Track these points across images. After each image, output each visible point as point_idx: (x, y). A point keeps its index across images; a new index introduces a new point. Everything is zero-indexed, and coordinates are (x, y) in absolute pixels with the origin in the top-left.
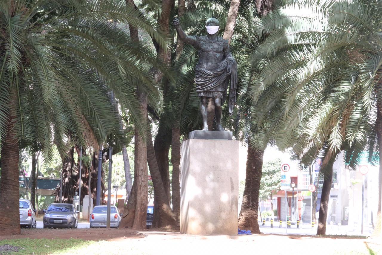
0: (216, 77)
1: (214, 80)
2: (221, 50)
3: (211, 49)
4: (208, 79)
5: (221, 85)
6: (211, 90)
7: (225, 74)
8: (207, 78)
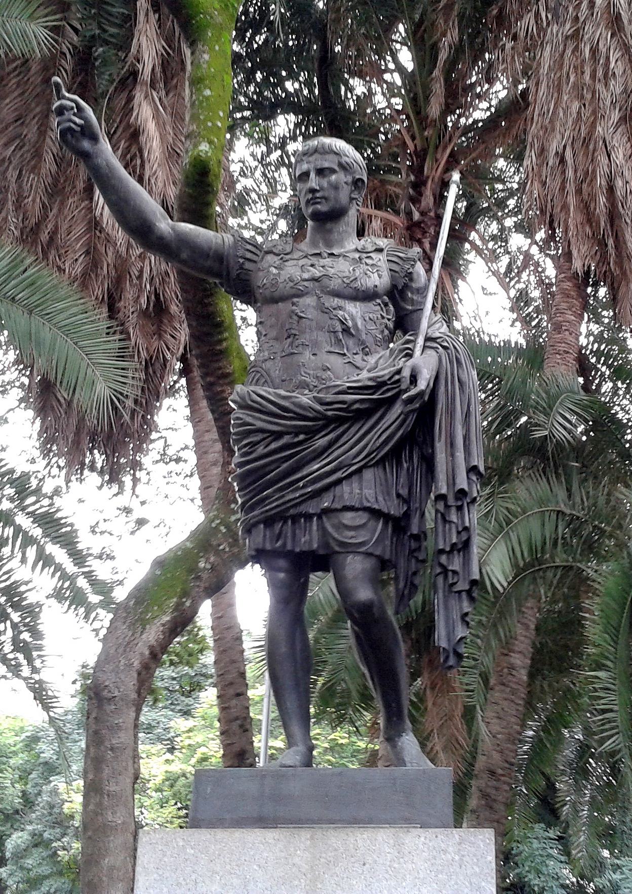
0: (338, 421)
1: (321, 442)
4: (286, 439)
5: (368, 474)
6: (302, 509)
8: (278, 435)
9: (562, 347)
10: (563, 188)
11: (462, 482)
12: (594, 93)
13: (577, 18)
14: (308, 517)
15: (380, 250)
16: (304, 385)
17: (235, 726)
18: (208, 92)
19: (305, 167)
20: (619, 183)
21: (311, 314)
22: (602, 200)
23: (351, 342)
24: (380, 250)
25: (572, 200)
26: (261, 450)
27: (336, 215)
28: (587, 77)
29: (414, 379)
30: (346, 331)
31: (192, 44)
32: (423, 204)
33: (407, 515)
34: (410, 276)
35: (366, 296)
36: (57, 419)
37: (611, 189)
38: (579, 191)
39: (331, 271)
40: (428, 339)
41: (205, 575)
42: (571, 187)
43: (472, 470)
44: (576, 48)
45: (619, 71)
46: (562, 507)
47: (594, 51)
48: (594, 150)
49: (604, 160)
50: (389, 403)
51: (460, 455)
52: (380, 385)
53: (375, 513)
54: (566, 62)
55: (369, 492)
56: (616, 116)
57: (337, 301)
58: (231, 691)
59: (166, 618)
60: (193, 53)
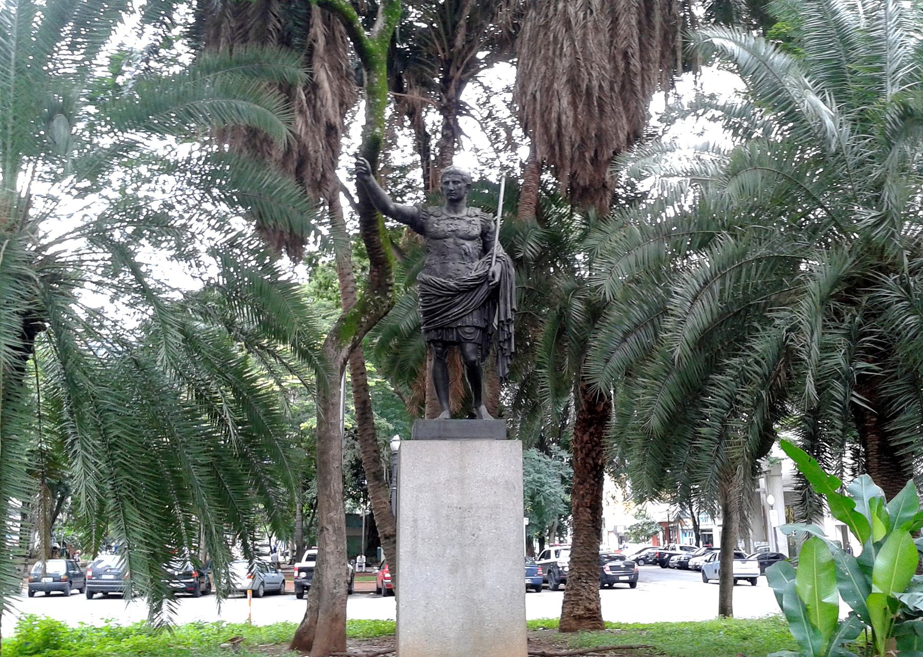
0: (464, 292)
2: (477, 231)
3: (452, 231)
5: (475, 313)
6: (450, 326)
7: (485, 287)
8: (440, 297)
9: (529, 200)
10: (534, 113)
11: (509, 316)
12: (554, 62)
13: (547, 16)
14: (452, 328)
15: (477, 216)
16: (450, 277)
17: (361, 388)
18: (378, 100)
19: (448, 179)
20: (564, 118)
21: (452, 246)
22: (554, 125)
23: (467, 258)
24: (477, 216)
25: (538, 121)
26: (434, 302)
27: (459, 200)
28: (551, 53)
29: (493, 276)
30: (466, 254)
31: (368, 70)
32: (449, 94)
33: (487, 327)
34: (489, 228)
35: (471, 239)
36: (268, 234)
37: (559, 120)
38: (543, 116)
39: (460, 227)
40: (497, 257)
41: (364, 325)
42: (538, 113)
43: (513, 310)
44: (545, 34)
45: (568, 54)
46: (525, 285)
47: (555, 38)
48: (552, 96)
49: (556, 103)
50: (482, 284)
51: (509, 305)
52: (479, 277)
53: (477, 328)
54: (539, 41)
55: (475, 320)
56: (564, 79)
57: (462, 241)
58: (359, 372)
59: (350, 345)
60: (368, 75)
